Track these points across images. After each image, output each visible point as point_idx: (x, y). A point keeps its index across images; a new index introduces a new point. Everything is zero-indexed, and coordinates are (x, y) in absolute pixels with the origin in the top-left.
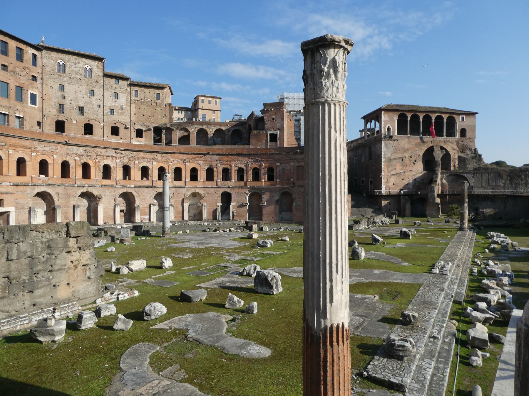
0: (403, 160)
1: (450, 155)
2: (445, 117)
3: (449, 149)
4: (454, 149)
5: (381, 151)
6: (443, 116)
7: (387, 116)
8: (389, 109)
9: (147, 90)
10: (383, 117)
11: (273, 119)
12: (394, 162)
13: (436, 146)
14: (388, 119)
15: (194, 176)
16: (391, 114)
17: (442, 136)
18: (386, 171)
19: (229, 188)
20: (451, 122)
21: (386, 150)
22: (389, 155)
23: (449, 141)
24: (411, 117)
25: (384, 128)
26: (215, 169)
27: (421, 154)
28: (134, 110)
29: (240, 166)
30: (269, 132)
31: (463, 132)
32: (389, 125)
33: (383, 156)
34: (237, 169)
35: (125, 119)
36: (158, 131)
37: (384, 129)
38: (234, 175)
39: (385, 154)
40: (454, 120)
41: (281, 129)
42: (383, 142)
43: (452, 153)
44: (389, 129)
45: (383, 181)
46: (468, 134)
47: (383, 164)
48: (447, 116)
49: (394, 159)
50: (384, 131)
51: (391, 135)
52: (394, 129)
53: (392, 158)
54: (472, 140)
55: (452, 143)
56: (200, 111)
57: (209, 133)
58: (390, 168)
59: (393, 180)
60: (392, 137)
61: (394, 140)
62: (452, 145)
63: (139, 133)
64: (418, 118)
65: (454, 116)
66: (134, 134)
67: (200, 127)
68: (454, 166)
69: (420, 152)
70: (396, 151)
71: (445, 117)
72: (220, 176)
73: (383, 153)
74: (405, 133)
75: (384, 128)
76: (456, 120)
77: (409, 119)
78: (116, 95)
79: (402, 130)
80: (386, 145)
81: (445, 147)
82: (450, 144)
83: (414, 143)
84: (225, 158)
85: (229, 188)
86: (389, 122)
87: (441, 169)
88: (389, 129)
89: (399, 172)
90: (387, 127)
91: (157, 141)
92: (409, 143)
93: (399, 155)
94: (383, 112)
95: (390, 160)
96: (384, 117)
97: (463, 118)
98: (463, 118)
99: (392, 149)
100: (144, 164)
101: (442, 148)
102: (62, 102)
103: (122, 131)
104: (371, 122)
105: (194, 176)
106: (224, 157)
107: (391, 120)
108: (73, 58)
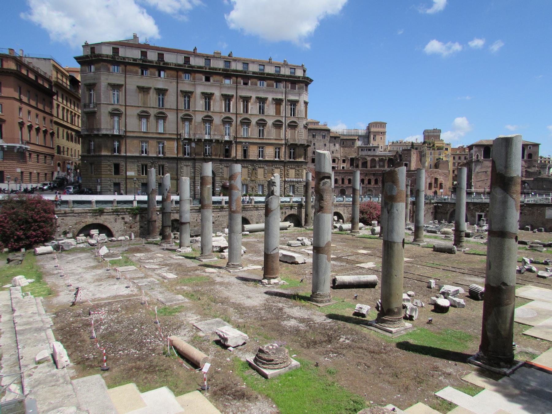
8: (477, 146)
9: (348, 142)
12: (480, 174)
15: (369, 183)
28: (342, 150)
30: (404, 163)
35: (338, 155)
36: (352, 160)
41: (410, 162)
47: (473, 175)
56: (372, 133)
58: (478, 177)
59: (479, 184)
63: (344, 161)
66: (342, 161)
78: (335, 145)
91: (352, 164)
95: (478, 173)
97: (530, 148)
98: (530, 148)
100: (349, 177)
102: (314, 150)
103: (337, 161)
105: (369, 183)
107: (480, 151)
108: (318, 132)
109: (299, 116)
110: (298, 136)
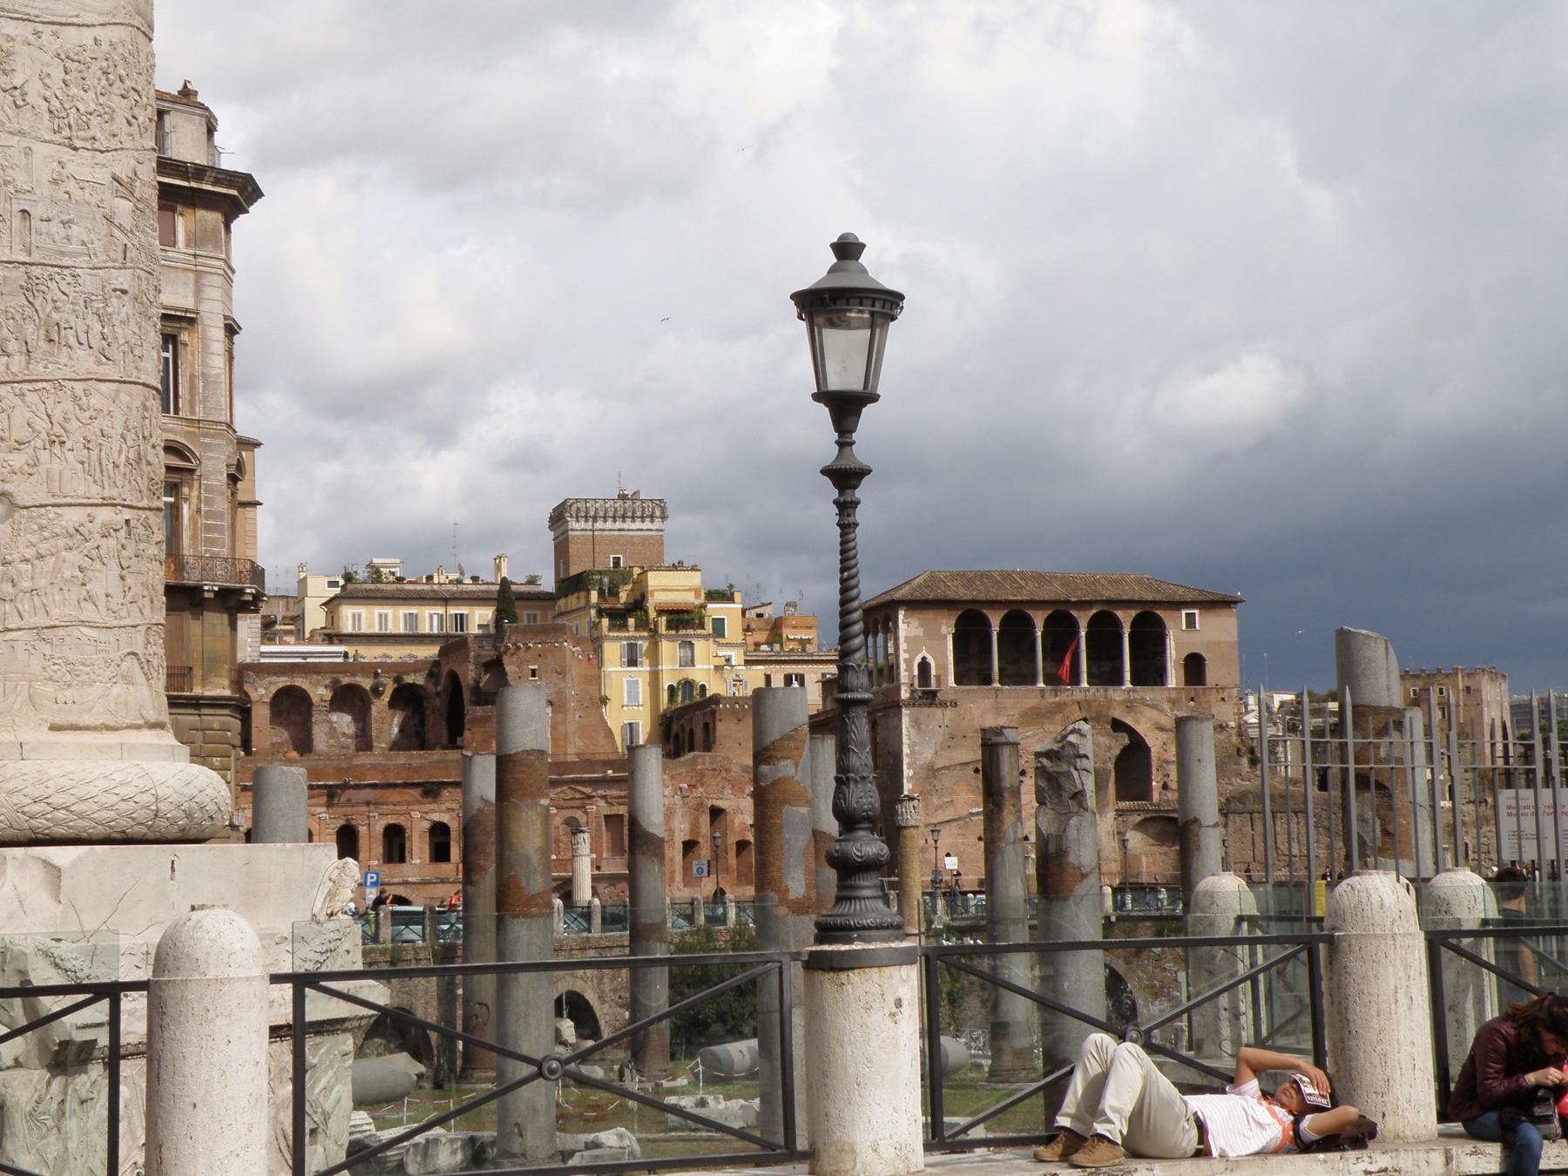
1: (1148, 749)
2: (1126, 618)
3: (1142, 729)
4: (1162, 729)
5: (900, 743)
6: (1119, 614)
7: (915, 622)
10: (902, 627)
11: (534, 673)
12: (947, 779)
14: (920, 632)
16: (930, 615)
17: (1120, 682)
19: (405, 883)
20: (1150, 636)
21: (916, 739)
22: (927, 755)
23: (1143, 702)
24: (1003, 623)
25: (909, 662)
26: (363, 830)
29: (436, 817)
31: (1194, 667)
32: (924, 653)
33: (906, 760)
34: (426, 825)
37: (909, 669)
38: (419, 847)
40: (1160, 624)
42: (905, 711)
43: (1154, 740)
44: (924, 666)
46: (1212, 674)
48: (1133, 613)
50: (907, 675)
51: (933, 687)
52: (942, 667)
54: (1225, 695)
55: (1154, 707)
57: (315, 700)
60: (934, 693)
61: (943, 705)
62: (1155, 714)
64: (1030, 623)
67: (283, 681)
68: (1165, 787)
71: (1126, 618)
72: (379, 849)
73: (906, 750)
74: (986, 680)
75: (909, 662)
76: (1168, 623)
77: (995, 629)
79: (971, 667)
80: (916, 723)
81: (1128, 721)
82: (1148, 712)
83: (1017, 712)
84: (394, 796)
85: (405, 883)
86: (922, 644)
87: (1120, 797)
88: (924, 666)
89: (964, 813)
90: (918, 660)
92: (998, 709)
94: (901, 614)
95: (932, 772)
96: (907, 626)
97: (1190, 617)
98: (1190, 617)
99: (940, 734)
101: (1118, 726)
104: (875, 636)
106: (389, 792)
107: (933, 636)
109: (200, 414)
110: (194, 538)
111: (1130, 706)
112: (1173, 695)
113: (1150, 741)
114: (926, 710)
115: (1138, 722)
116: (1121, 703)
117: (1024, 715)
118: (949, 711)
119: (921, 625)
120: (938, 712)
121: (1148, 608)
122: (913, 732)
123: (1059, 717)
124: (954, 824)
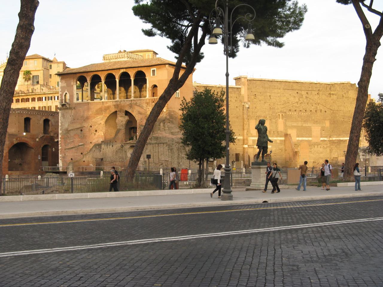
0: (82, 130)
1: (136, 121)
6: (130, 73)
7: (64, 81)
12: (72, 134)
13: (120, 111)
14: (65, 85)
18: (63, 145)
20: (141, 79)
22: (66, 126)
27: (103, 122)
32: (66, 92)
33: (60, 128)
39: (62, 125)
45: (60, 155)
49: (72, 130)
52: (72, 96)
53: (70, 129)
55: (139, 106)
61: (70, 108)
65: (143, 70)
69: (102, 119)
70: (74, 120)
73: (60, 124)
76: (147, 74)
80: (63, 116)
81: (130, 111)
82: (136, 107)
89: (77, 145)
90: (64, 94)
93: (79, 126)
95: (67, 131)
97: (154, 71)
98: (154, 71)
99: (70, 119)
101: (127, 113)
111: (131, 106)
112: (148, 101)
113: (137, 118)
114: (67, 111)
115: (133, 111)
116: (128, 105)
117: (97, 111)
118: (73, 111)
119: (65, 82)
120: (70, 111)
121: (140, 69)
122: (62, 119)
123: (108, 111)
124: (74, 149)
